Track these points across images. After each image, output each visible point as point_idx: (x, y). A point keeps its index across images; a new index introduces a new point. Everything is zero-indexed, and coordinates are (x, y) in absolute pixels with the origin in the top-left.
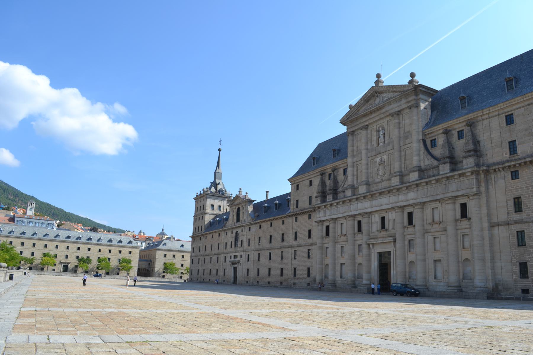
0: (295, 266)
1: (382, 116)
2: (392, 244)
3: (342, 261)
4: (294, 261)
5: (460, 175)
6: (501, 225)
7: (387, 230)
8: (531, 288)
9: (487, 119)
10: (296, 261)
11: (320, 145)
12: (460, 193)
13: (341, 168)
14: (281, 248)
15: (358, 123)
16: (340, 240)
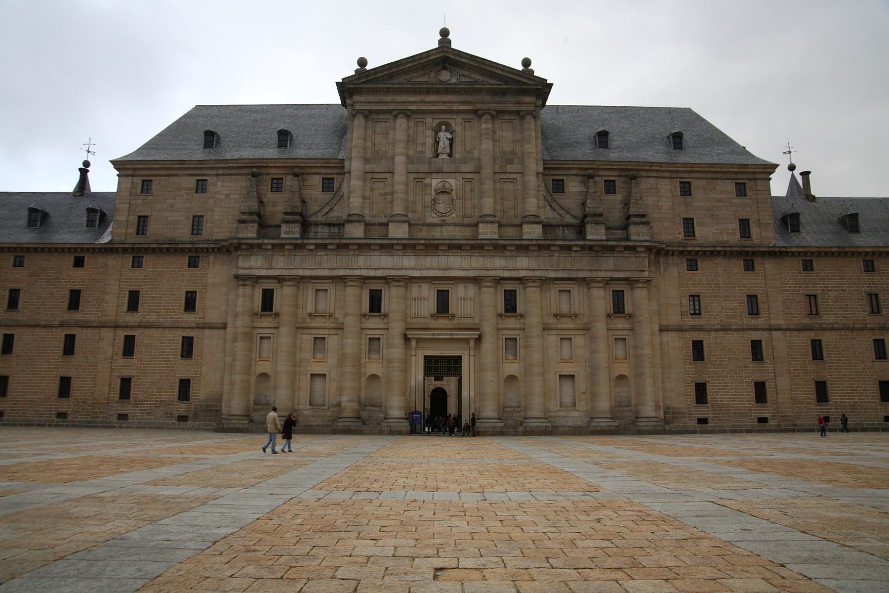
0: (126, 373)
1: (455, 107)
2: (472, 343)
3: (317, 369)
4: (121, 361)
5: (627, 248)
6: (672, 330)
7: (453, 316)
8: (710, 416)
9: (654, 177)
10: (133, 361)
11: (199, 109)
12: (622, 275)
13: (316, 174)
14: (62, 325)
15: (389, 99)
16: (313, 325)
